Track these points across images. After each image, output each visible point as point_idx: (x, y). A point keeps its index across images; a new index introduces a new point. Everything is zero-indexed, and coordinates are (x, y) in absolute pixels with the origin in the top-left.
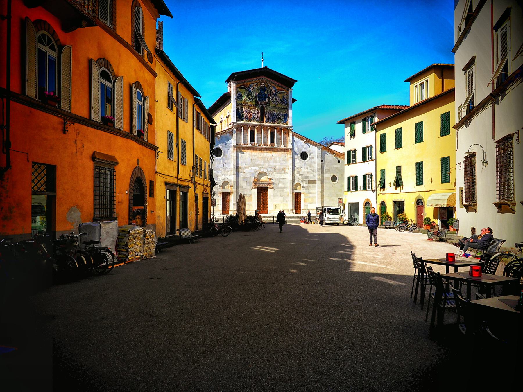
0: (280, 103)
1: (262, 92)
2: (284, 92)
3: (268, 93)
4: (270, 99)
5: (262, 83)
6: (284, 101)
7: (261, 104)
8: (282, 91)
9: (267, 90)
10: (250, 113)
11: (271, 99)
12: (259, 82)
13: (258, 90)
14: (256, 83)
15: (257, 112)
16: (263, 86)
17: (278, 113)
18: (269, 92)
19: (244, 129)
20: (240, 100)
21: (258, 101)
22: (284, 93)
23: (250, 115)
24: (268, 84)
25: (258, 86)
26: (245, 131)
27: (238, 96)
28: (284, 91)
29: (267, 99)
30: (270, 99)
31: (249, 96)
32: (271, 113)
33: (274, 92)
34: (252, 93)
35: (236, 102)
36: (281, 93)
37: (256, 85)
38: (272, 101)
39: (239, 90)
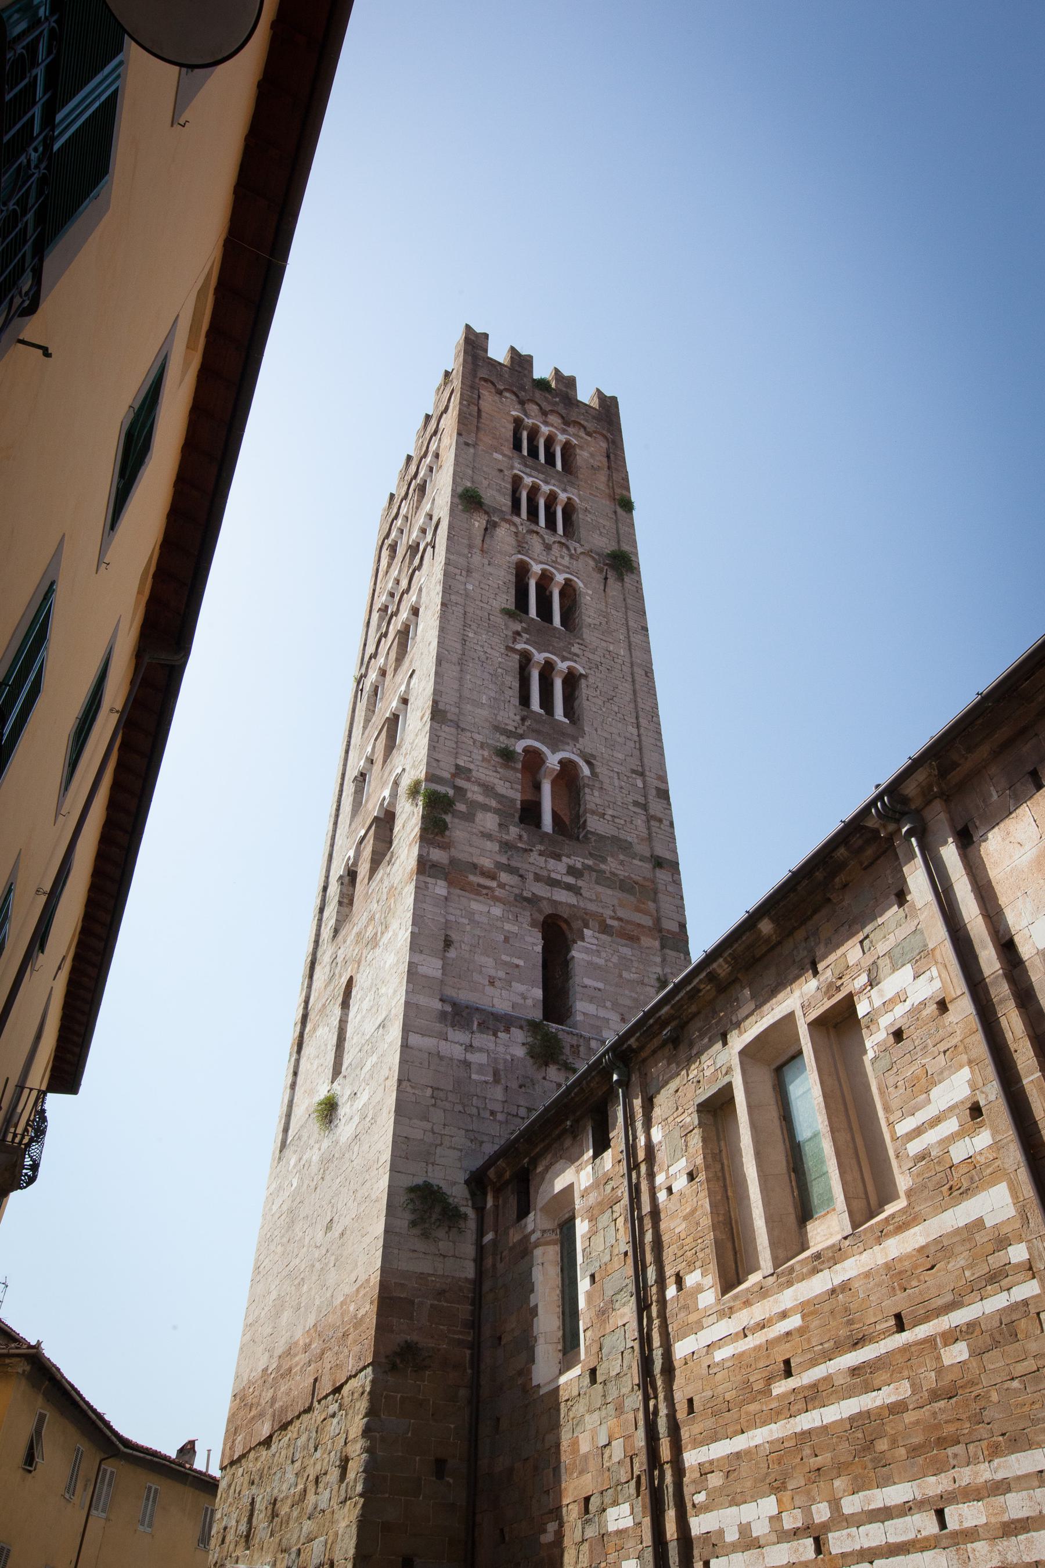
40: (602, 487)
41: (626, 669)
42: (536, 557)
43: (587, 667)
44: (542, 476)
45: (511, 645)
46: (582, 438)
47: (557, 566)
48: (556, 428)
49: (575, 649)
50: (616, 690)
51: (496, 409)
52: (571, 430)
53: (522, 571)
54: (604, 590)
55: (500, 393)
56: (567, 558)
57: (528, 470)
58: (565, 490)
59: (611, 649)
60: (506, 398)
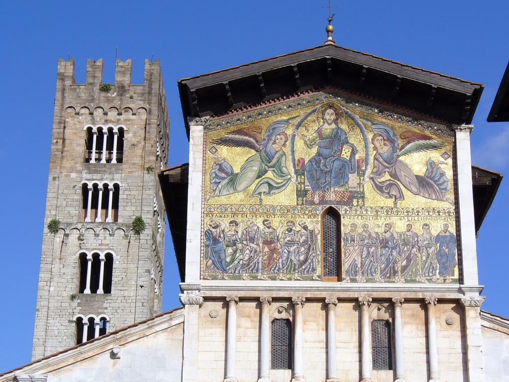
0: (415, 190)
1: (326, 152)
2: (432, 142)
3: (354, 152)
4: (367, 179)
5: (327, 117)
6: (431, 179)
7: (322, 202)
8: (422, 142)
9: (351, 141)
10: (267, 243)
11: (372, 179)
12: (314, 111)
13: (309, 146)
14: (299, 120)
15: (304, 238)
16: (333, 126)
17: (409, 233)
18: (360, 147)
19: (240, 315)
20: (224, 192)
21: (306, 191)
22: (434, 147)
23: (273, 251)
24: (353, 119)
25: (308, 130)
26: (246, 323)
27: (217, 176)
28: (429, 138)
29: (353, 179)
30: (367, 179)
31: (270, 174)
32: (374, 235)
33: (385, 150)
34: (282, 156)
35: (205, 200)
36: (419, 148)
37: (299, 126)
38: (376, 185)
39: (224, 151)
40: (138, 160)
41: (133, 305)
42: (90, 247)
43: (111, 314)
44: (99, 176)
45: (71, 319)
46: (129, 120)
47: (102, 247)
48: (113, 122)
49: (105, 305)
50: (125, 322)
51: (74, 131)
52: (122, 118)
53: (83, 257)
54: (128, 251)
55: (78, 114)
56: (108, 237)
57: (89, 176)
58: (113, 179)
59: (126, 293)
60: (82, 114)
